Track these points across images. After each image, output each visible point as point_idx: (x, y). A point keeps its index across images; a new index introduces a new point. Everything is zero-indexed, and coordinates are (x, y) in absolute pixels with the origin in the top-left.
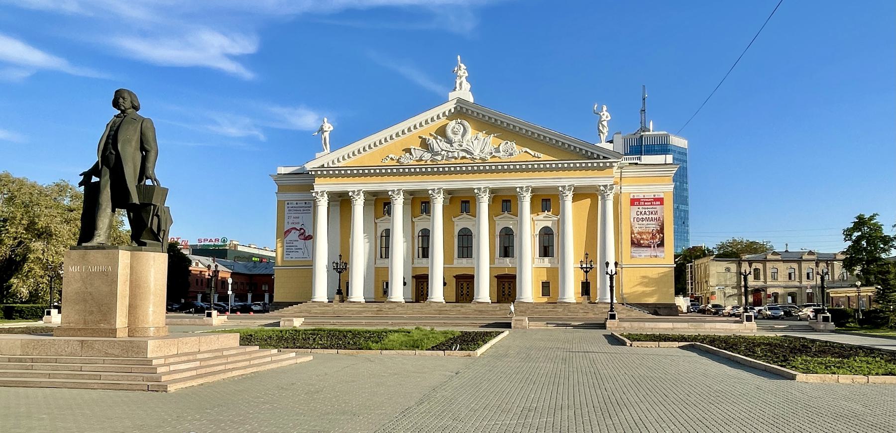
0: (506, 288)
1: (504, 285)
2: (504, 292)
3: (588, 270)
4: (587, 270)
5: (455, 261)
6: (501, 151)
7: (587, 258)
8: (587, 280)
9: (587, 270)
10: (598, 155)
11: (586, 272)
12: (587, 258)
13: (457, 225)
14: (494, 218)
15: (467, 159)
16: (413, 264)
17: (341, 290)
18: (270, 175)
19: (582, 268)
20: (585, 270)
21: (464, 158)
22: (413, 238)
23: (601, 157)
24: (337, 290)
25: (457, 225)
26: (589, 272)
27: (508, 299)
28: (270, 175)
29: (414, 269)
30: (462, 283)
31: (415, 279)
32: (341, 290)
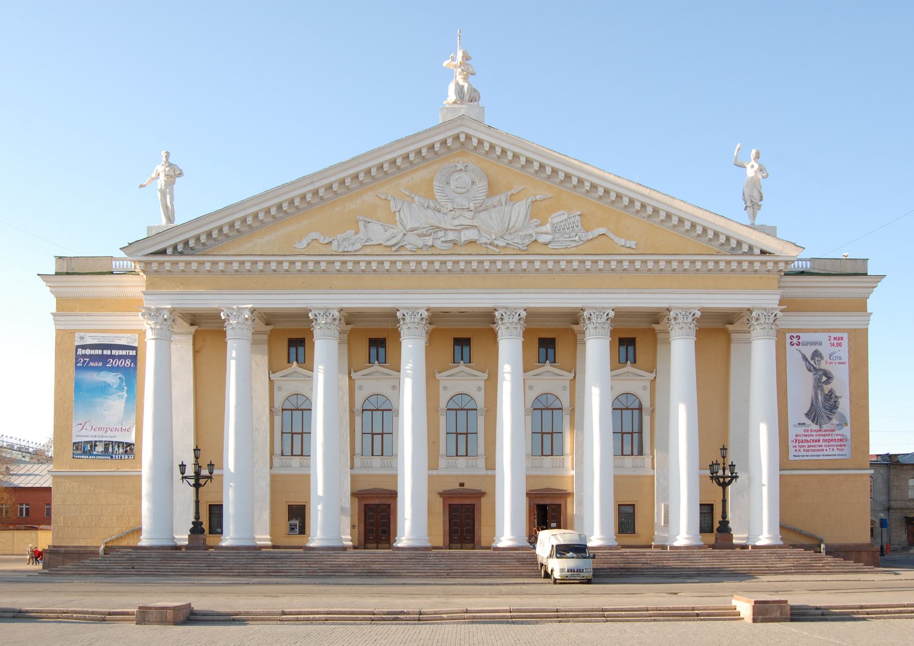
4: (724, 482)
7: (724, 457)
9: (724, 482)
12: (724, 457)
16: (352, 468)
19: (714, 477)
20: (721, 480)
22: (352, 412)
24: (193, 523)
25: (445, 388)
29: (354, 478)
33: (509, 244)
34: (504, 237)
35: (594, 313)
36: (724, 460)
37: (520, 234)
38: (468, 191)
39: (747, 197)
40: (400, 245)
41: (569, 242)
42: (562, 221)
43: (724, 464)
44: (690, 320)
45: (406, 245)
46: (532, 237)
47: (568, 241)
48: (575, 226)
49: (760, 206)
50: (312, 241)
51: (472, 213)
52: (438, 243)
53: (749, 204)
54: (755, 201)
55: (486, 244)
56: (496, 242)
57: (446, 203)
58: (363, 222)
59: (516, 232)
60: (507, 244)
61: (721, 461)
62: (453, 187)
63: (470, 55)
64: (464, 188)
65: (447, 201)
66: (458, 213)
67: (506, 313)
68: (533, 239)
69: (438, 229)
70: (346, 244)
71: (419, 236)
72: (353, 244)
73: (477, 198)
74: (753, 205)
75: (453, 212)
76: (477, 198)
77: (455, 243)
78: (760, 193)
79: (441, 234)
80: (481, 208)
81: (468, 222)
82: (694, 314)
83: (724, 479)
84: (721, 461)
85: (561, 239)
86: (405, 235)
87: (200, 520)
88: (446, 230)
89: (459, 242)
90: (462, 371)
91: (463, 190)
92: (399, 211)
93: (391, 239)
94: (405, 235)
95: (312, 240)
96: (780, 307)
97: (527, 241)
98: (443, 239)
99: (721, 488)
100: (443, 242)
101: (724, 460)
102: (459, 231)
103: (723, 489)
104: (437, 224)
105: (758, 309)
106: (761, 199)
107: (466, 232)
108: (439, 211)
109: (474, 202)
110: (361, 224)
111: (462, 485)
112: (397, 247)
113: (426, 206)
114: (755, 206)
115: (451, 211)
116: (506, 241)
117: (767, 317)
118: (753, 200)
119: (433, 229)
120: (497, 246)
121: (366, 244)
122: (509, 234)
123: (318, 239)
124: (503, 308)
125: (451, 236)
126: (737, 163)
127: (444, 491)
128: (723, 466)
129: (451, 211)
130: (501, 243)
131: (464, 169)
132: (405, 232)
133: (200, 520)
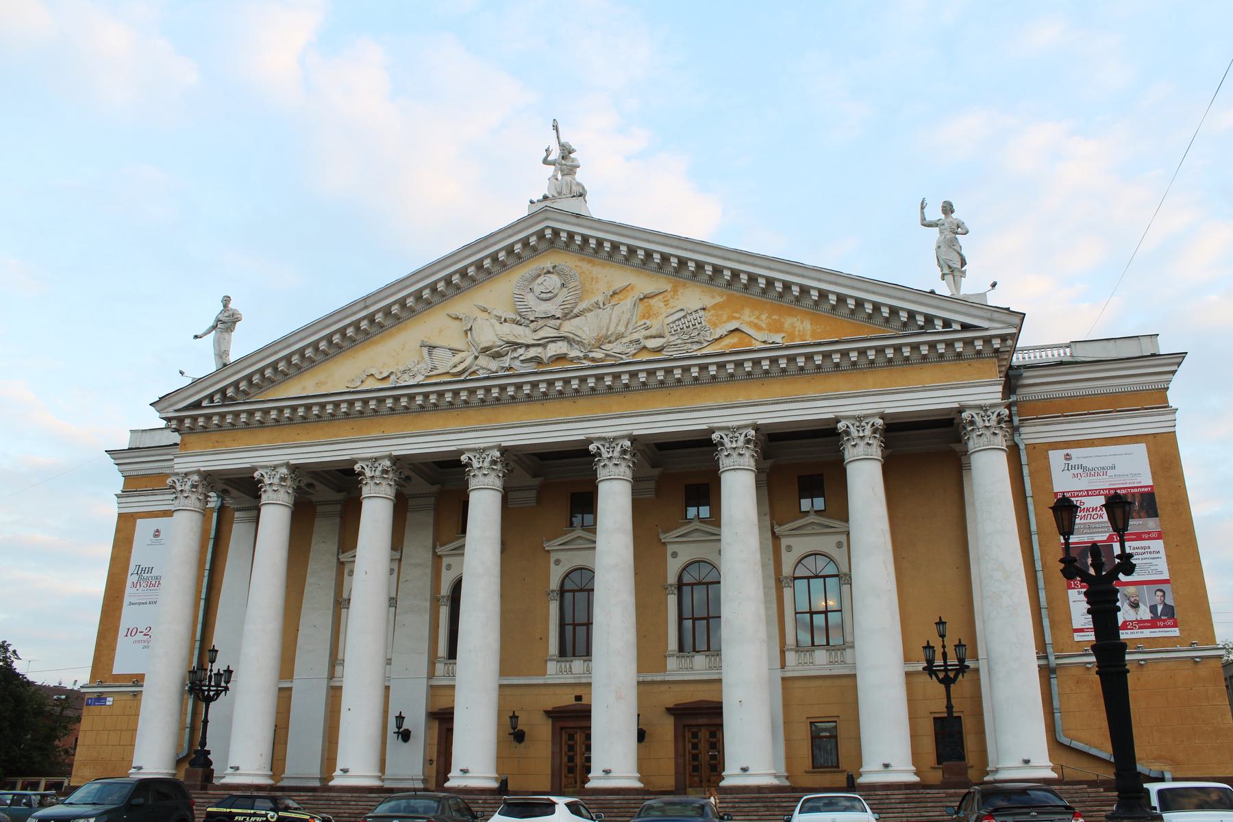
0: (703, 745)
1: (695, 735)
2: (695, 757)
3: (951, 675)
4: (947, 676)
5: (552, 667)
6: (667, 334)
7: (942, 636)
8: (949, 707)
9: (947, 676)
10: (947, 323)
11: (947, 682)
12: (942, 636)
13: (557, 562)
14: (662, 536)
15: (572, 360)
17: (208, 752)
18: (106, 451)
20: (941, 675)
21: (561, 358)
23: (957, 327)
26: (954, 680)
27: (709, 781)
28: (106, 451)
30: (571, 731)
31: (436, 725)
32: (208, 752)
33: (610, 356)
34: (602, 347)
35: (727, 435)
36: (943, 641)
37: (624, 340)
38: (555, 296)
39: (942, 262)
40: (470, 371)
41: (690, 345)
42: (680, 319)
43: (944, 647)
44: (868, 432)
45: (478, 370)
46: (640, 344)
47: (688, 343)
48: (697, 323)
49: (964, 272)
50: (366, 378)
51: (559, 321)
52: (516, 364)
53: (946, 271)
54: (955, 266)
55: (578, 358)
56: (591, 355)
57: (526, 313)
58: (426, 349)
59: (617, 339)
60: (607, 355)
61: (936, 643)
62: (537, 294)
63: (573, 147)
64: (550, 292)
65: (529, 310)
66: (541, 323)
67: (603, 446)
68: (642, 344)
69: (515, 345)
70: (406, 376)
71: (494, 358)
72: (414, 376)
73: (566, 303)
74: (952, 271)
75: (535, 323)
76: (566, 303)
77: (537, 360)
78: (961, 255)
79: (521, 351)
80: (572, 314)
81: (553, 333)
82: (873, 425)
83: (946, 673)
84: (936, 643)
85: (679, 341)
86: (476, 358)
87: (206, 748)
88: (528, 346)
89: (543, 357)
90: (579, 537)
91: (549, 295)
92: (471, 329)
93: (459, 364)
94: (476, 358)
95: (368, 376)
96: (1003, 401)
97: (632, 350)
98: (521, 358)
99: (942, 686)
100: (521, 361)
101: (943, 641)
102: (544, 346)
103: (946, 687)
104: (512, 339)
105: (971, 407)
106: (963, 263)
107: (551, 346)
108: (521, 325)
109: (562, 307)
110: (425, 350)
111: (578, 698)
112: (467, 373)
113: (503, 320)
114: (956, 273)
115: (532, 321)
116: (604, 352)
117: (986, 418)
118: (951, 264)
119: (510, 346)
120: (593, 360)
121: (429, 374)
122: (609, 342)
123: (374, 373)
124: (599, 439)
125: (533, 352)
126: (925, 222)
127: (553, 708)
128: (942, 650)
129: (532, 321)
130: (598, 355)
131: (552, 270)
132: (477, 354)
133: (206, 748)
